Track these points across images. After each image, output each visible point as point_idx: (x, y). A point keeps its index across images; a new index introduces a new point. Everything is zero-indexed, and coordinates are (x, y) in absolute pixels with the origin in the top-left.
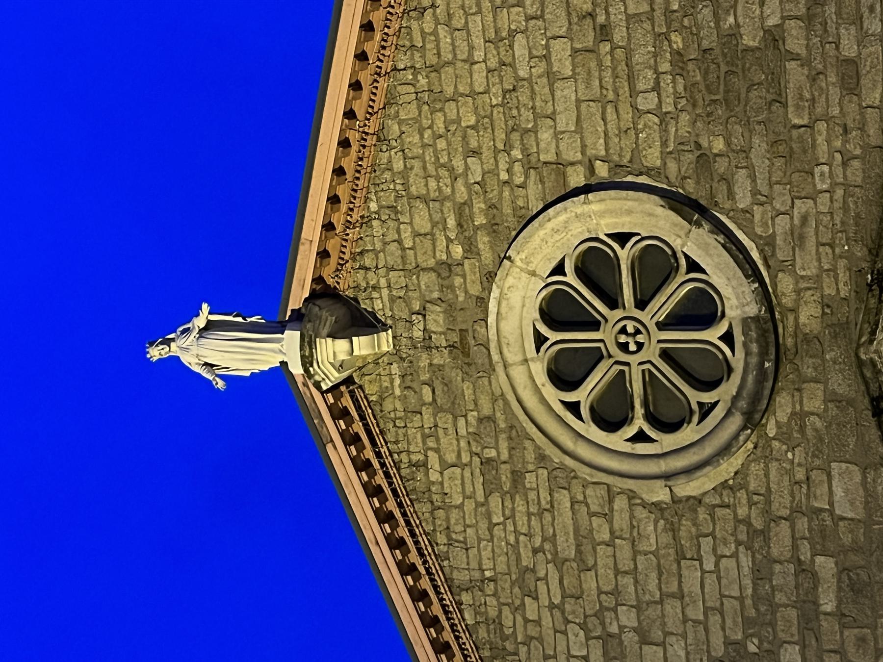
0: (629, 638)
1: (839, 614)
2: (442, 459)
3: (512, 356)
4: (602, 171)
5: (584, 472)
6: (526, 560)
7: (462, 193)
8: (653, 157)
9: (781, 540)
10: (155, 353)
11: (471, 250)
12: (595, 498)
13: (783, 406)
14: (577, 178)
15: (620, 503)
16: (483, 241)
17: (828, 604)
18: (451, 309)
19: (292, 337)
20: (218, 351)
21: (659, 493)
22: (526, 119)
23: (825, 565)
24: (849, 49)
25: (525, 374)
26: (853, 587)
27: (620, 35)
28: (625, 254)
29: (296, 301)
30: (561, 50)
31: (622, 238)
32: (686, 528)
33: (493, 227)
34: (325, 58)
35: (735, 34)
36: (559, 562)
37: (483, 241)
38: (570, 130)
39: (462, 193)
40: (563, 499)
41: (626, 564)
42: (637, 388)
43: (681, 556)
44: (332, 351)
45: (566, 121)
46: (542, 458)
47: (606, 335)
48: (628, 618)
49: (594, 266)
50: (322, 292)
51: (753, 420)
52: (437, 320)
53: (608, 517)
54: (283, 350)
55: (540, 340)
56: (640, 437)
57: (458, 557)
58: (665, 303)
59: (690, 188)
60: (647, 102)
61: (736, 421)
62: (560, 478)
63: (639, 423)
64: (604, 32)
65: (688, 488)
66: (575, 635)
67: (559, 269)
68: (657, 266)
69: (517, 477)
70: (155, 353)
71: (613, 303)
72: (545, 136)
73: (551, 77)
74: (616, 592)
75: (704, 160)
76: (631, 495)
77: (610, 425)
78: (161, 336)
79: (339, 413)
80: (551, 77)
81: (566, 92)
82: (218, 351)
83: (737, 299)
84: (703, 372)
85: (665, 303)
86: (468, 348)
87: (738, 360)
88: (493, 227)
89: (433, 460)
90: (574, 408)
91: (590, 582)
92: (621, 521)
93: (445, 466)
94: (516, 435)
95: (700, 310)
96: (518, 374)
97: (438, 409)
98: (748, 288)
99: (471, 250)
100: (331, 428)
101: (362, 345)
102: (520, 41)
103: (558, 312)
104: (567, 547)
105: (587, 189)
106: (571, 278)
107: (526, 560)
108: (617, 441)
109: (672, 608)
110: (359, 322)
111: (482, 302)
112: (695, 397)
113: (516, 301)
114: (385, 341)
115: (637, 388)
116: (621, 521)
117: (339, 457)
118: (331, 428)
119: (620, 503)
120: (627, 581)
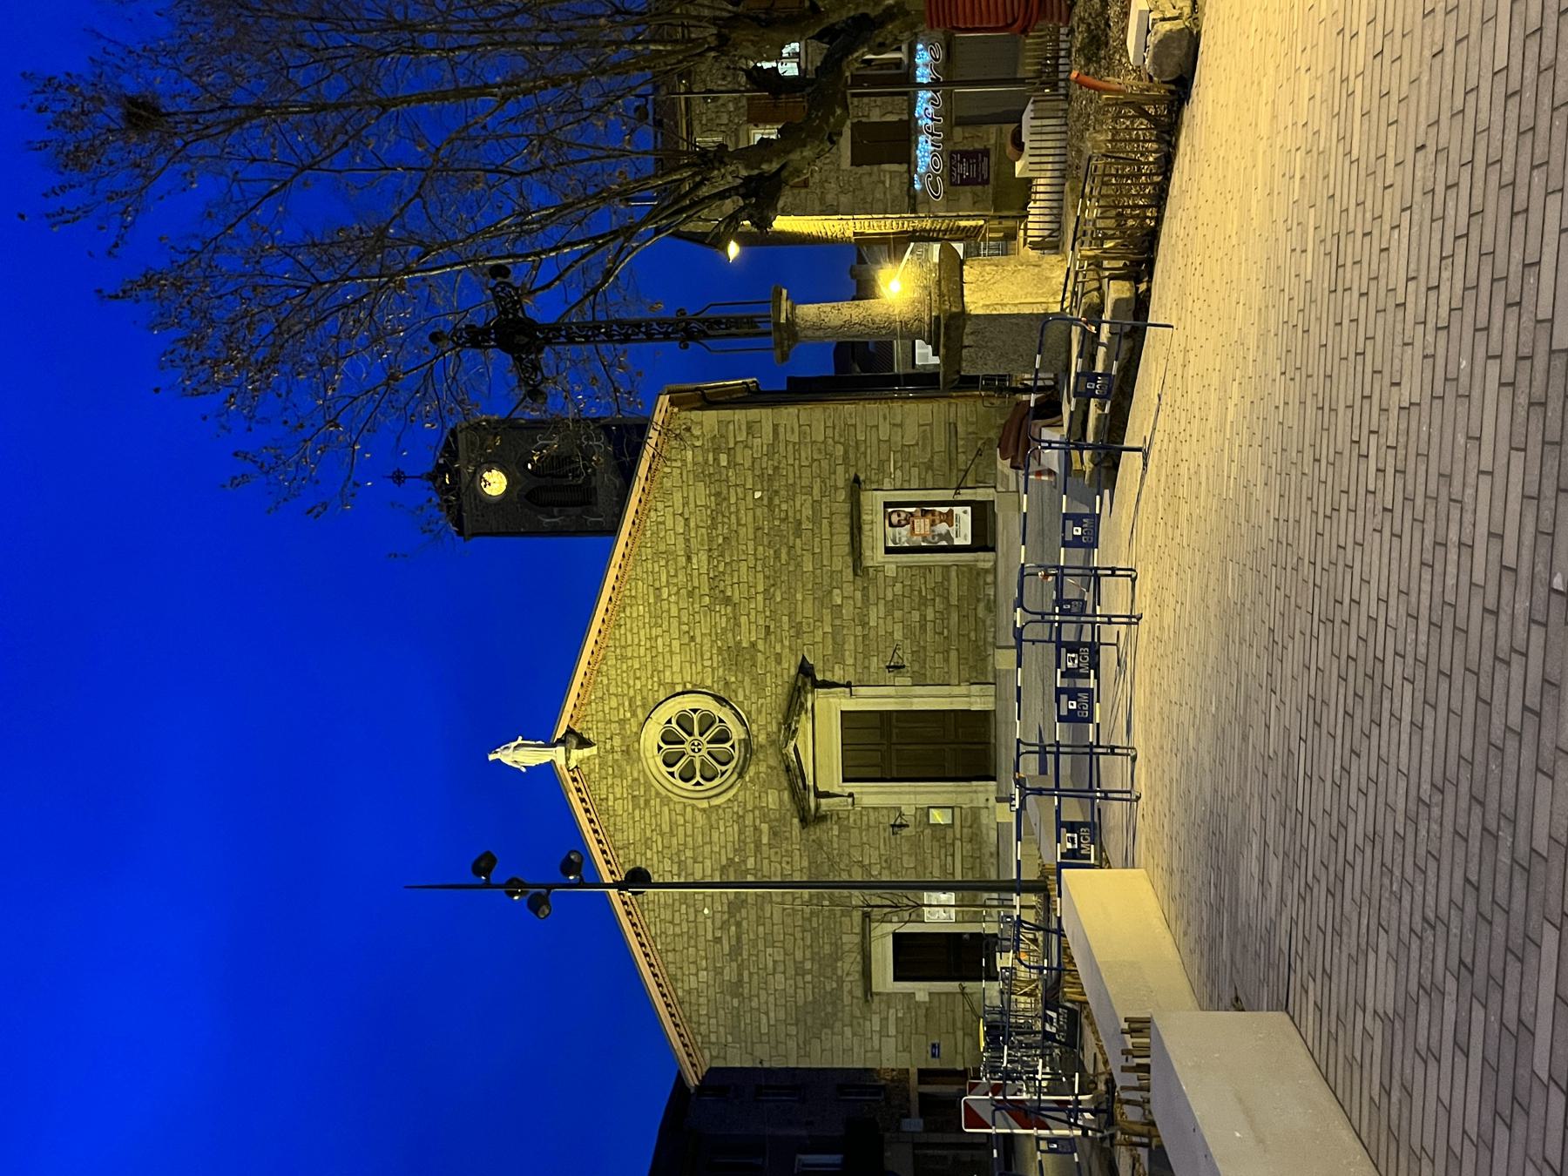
0: (690, 861)
1: (770, 846)
2: (617, 796)
3: (649, 755)
4: (689, 686)
5: (676, 799)
6: (648, 834)
7: (632, 693)
8: (709, 682)
9: (749, 821)
10: (492, 757)
11: (634, 714)
12: (679, 808)
13: (752, 770)
14: (679, 689)
15: (689, 809)
16: (639, 711)
17: (765, 840)
18: (623, 738)
19: (561, 749)
20: (520, 756)
21: (705, 804)
22: (661, 667)
23: (765, 827)
24: (778, 650)
25: (655, 763)
26: (774, 833)
27: (698, 640)
28: (695, 717)
29: (559, 734)
30: (676, 644)
31: (695, 711)
32: (714, 817)
33: (644, 706)
34: (959, 705)
35: (740, 642)
36: (662, 834)
37: (639, 711)
38: (678, 670)
39: (632, 693)
40: (666, 809)
41: (689, 832)
42: (698, 766)
43: (711, 827)
44: (577, 754)
45: (676, 668)
46: (658, 794)
47: (687, 747)
48: (689, 853)
49: (684, 721)
50: (570, 731)
51: (741, 776)
52: (617, 741)
53: (683, 815)
54: (557, 755)
55: (660, 748)
56: (698, 784)
57: (619, 836)
58: (710, 734)
59: (722, 694)
60: (707, 663)
61: (735, 776)
62: (666, 801)
63: (698, 778)
64: (692, 638)
65: (715, 802)
66: (667, 862)
67: (669, 722)
68: (708, 721)
69: (647, 802)
70: (492, 757)
71: (690, 734)
72: (668, 673)
73: (671, 652)
74: (685, 844)
75: (727, 683)
76: (693, 806)
77: (686, 780)
78: (493, 750)
79: (574, 780)
80: (671, 652)
81: (677, 658)
82: (520, 756)
83: (737, 733)
84: (723, 758)
85: (710, 734)
86: (630, 752)
87: (736, 755)
88: (644, 706)
89: (611, 797)
90: (672, 774)
91: (674, 840)
92: (689, 816)
93: (615, 799)
94: (648, 786)
95: (723, 737)
96: (651, 762)
97: (614, 776)
98: (742, 729)
99: (634, 714)
100: (572, 786)
101: (587, 752)
102: (660, 640)
103: (668, 738)
104: (666, 828)
105: (683, 693)
106: (674, 724)
107: (648, 834)
108: (689, 785)
109: (707, 848)
110: (584, 743)
111: (638, 736)
112: (719, 768)
113: (652, 734)
114: (594, 750)
115: (698, 766)
116: (689, 816)
117: (574, 798)
118: (572, 786)
119: (689, 809)
120: (689, 840)
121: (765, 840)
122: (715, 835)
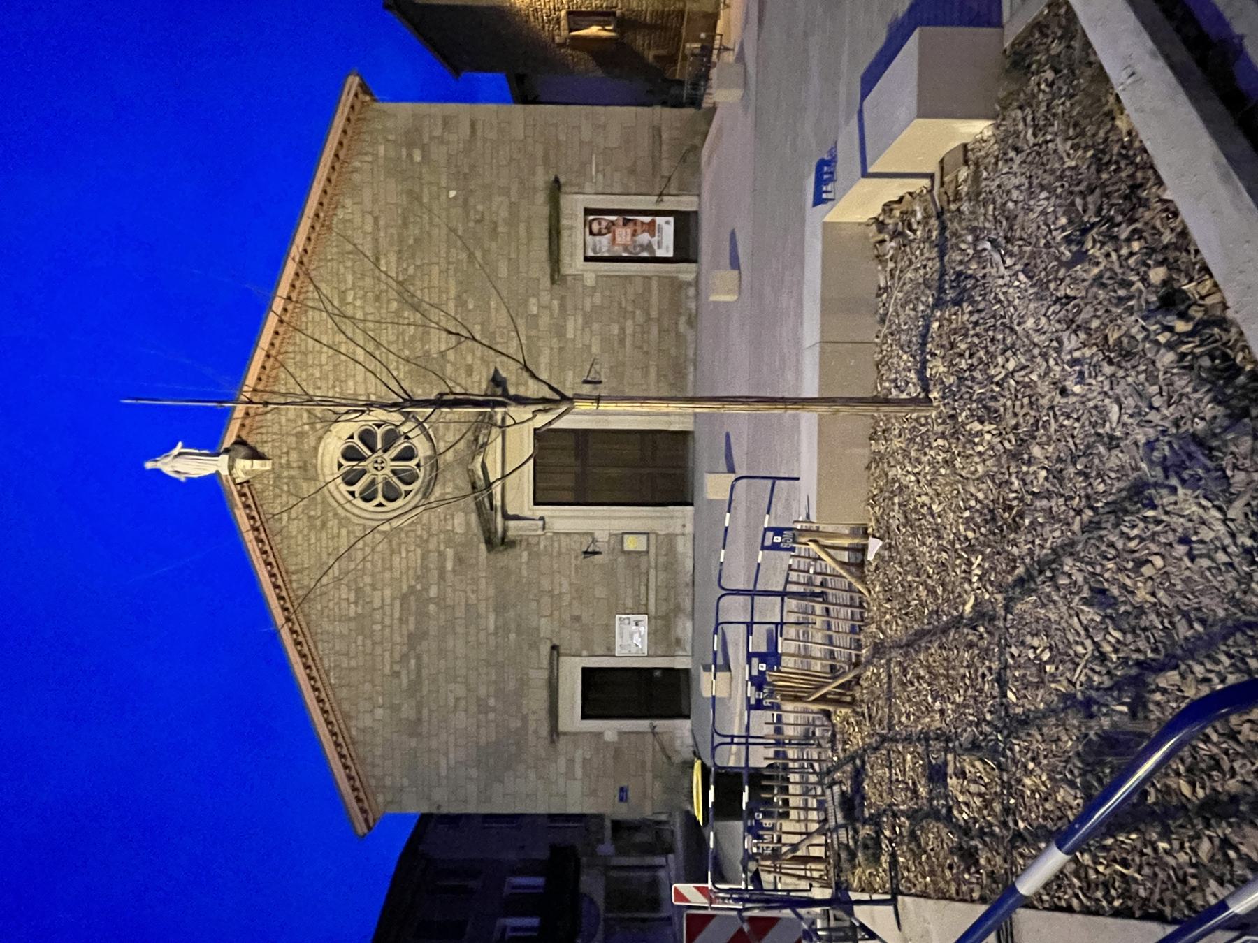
0: (368, 589)
1: (454, 571)
5: (355, 520)
9: (432, 545)
10: (149, 465)
13: (437, 492)
17: (449, 566)
19: (224, 459)
20: (182, 464)
21: (386, 527)
23: (450, 552)
24: (469, 359)
26: (459, 560)
32: (395, 541)
40: (344, 532)
42: (380, 487)
43: (393, 552)
44: (244, 466)
46: (336, 515)
48: (368, 580)
50: (240, 442)
51: (425, 496)
52: (294, 456)
54: (220, 464)
55: (340, 465)
56: (380, 505)
58: (394, 452)
61: (419, 496)
63: (380, 499)
65: (395, 523)
66: (344, 589)
69: (324, 524)
70: (149, 465)
71: (373, 451)
72: (351, 383)
74: (364, 569)
77: (367, 499)
78: (153, 456)
82: (182, 464)
83: (422, 448)
84: (408, 480)
85: (394, 452)
86: (308, 468)
87: (421, 474)
90: (352, 493)
95: (408, 454)
98: (428, 444)
100: (238, 501)
101: (257, 464)
103: (350, 454)
106: (356, 440)
108: (370, 506)
109: (387, 575)
110: (255, 455)
111: (316, 449)
112: (404, 488)
114: (267, 465)
115: (380, 487)
118: (238, 501)
121: (449, 566)
122: (396, 559)
